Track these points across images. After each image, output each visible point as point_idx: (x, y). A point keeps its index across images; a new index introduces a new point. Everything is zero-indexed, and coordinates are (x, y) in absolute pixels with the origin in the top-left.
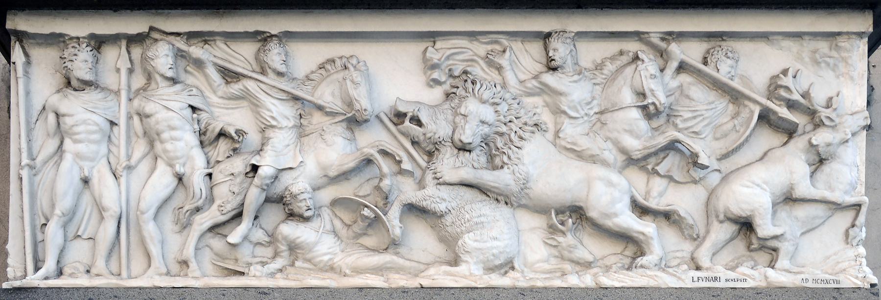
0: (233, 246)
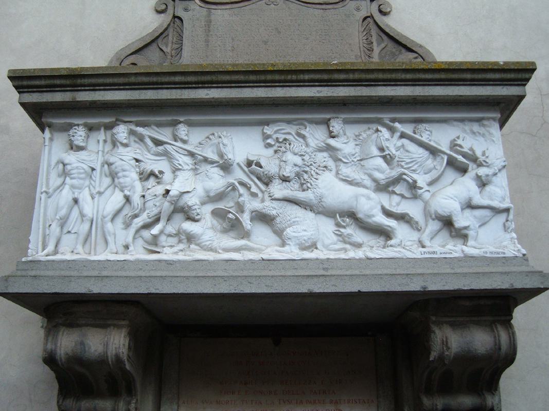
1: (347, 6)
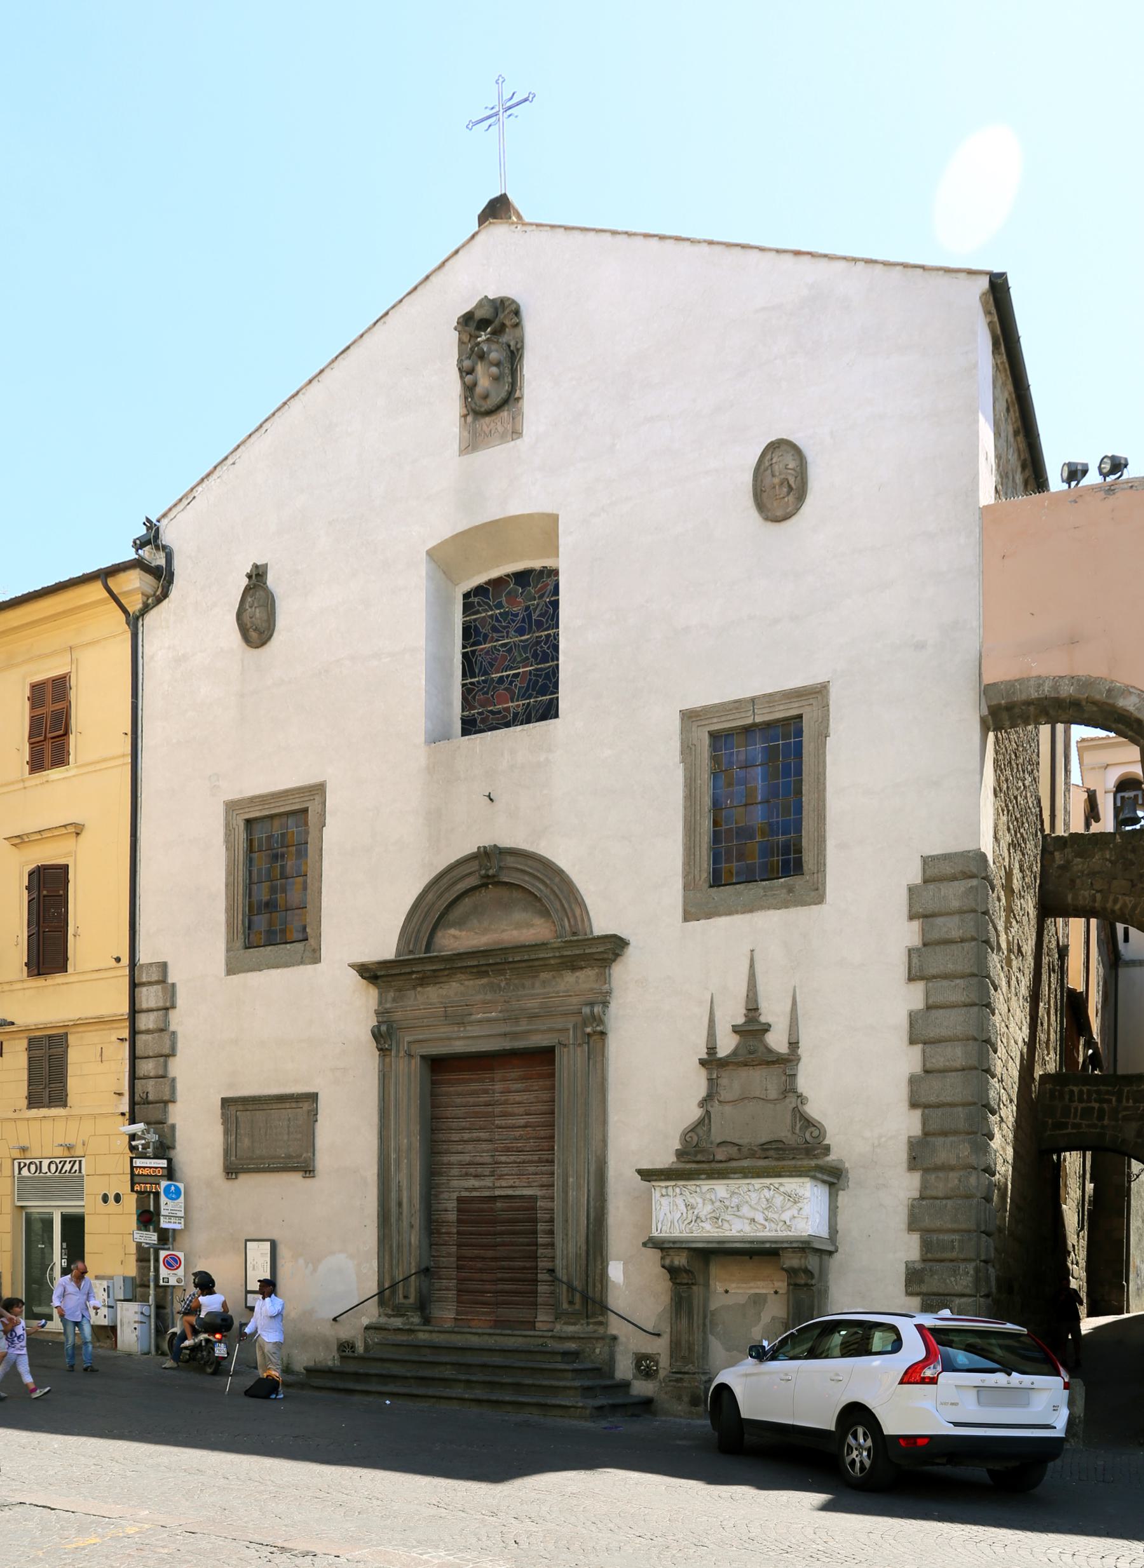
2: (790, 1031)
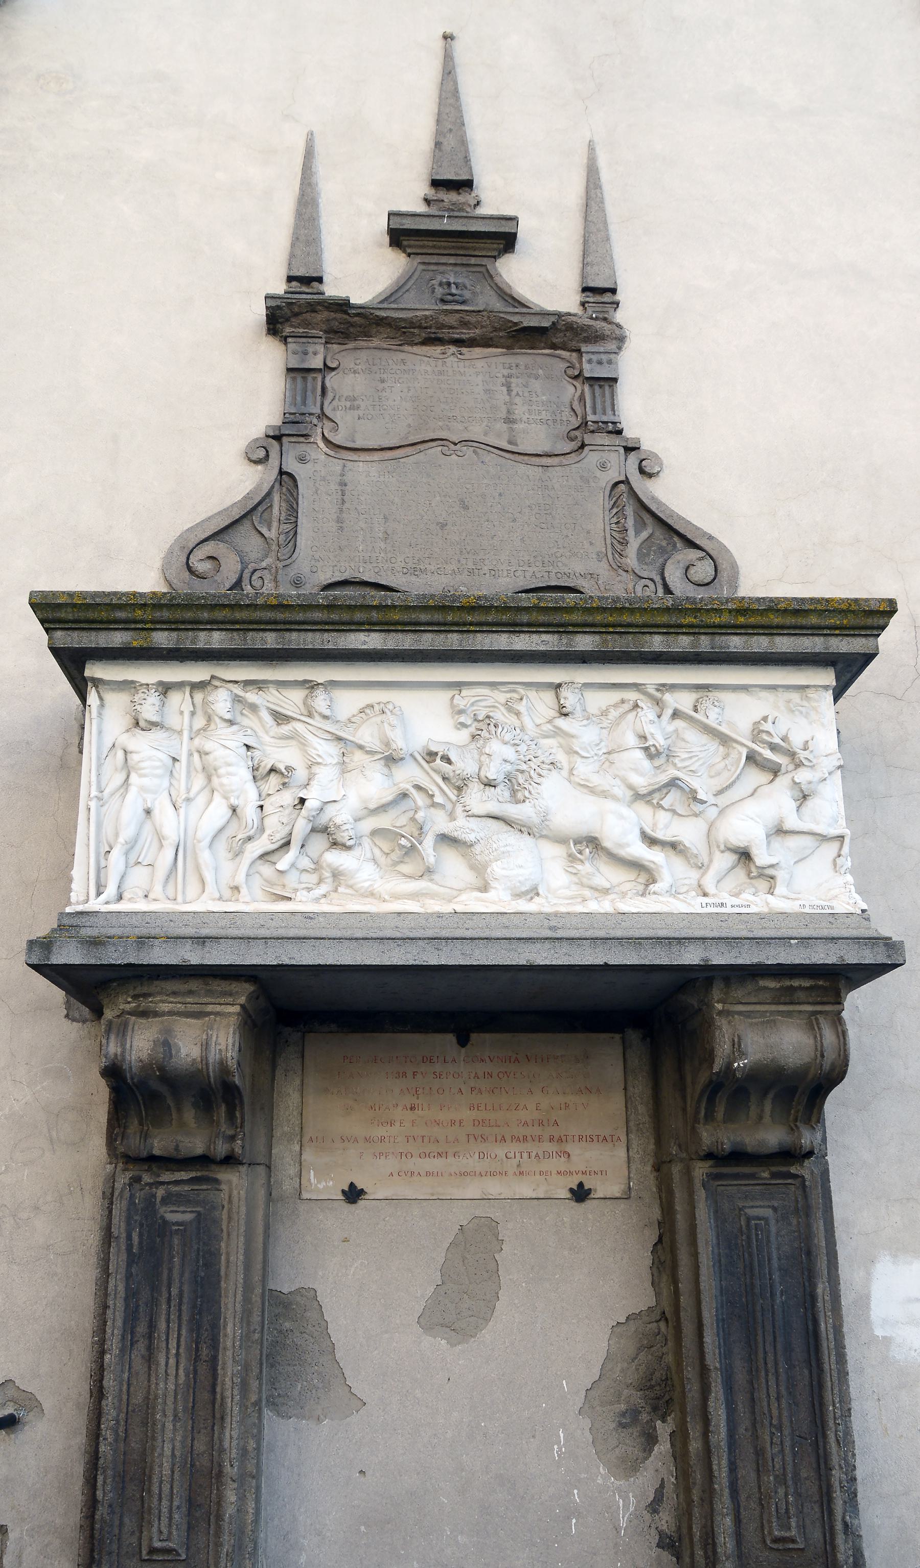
0: (281, 872)
1: (585, 461)
2: (585, 254)
